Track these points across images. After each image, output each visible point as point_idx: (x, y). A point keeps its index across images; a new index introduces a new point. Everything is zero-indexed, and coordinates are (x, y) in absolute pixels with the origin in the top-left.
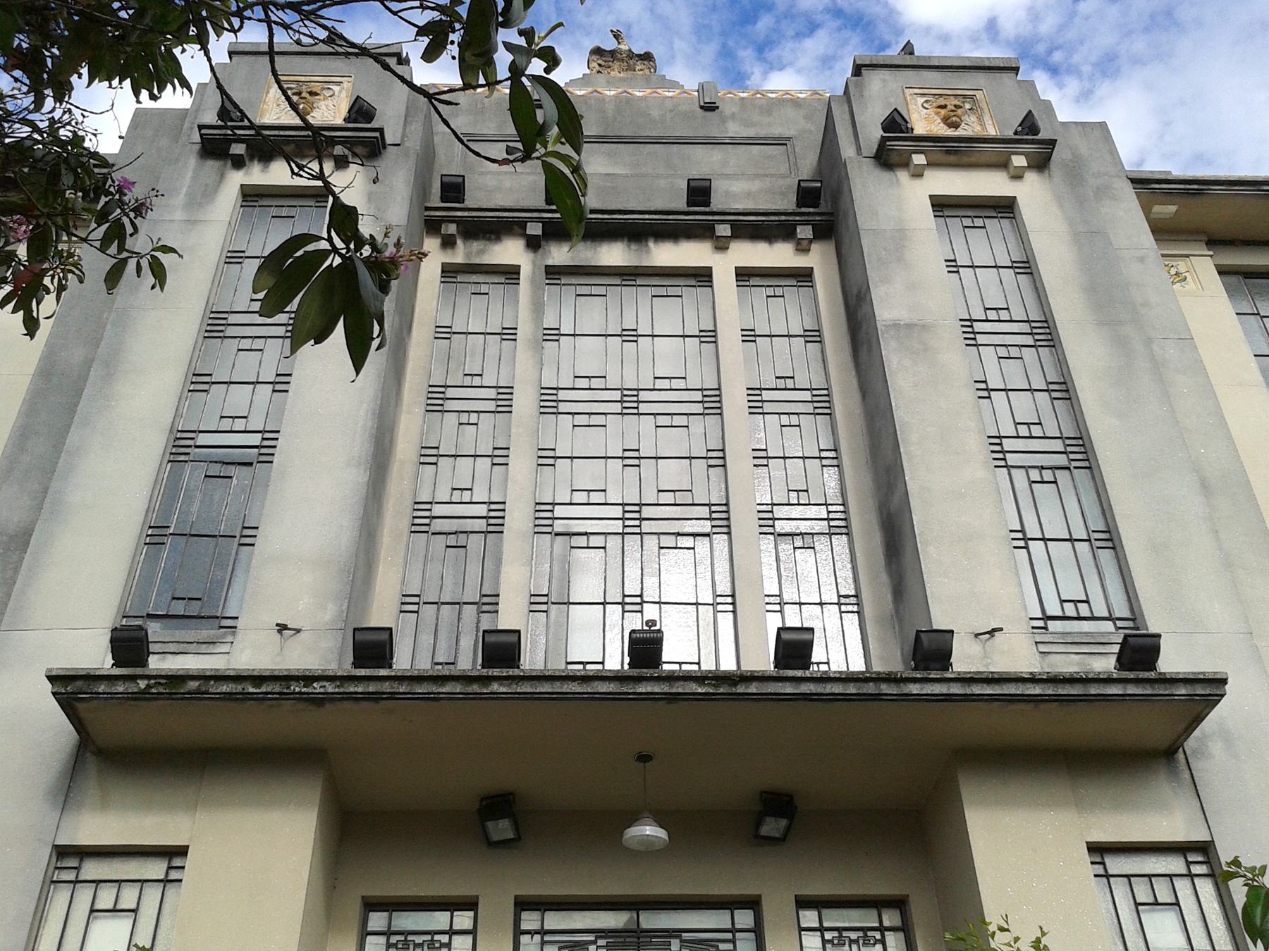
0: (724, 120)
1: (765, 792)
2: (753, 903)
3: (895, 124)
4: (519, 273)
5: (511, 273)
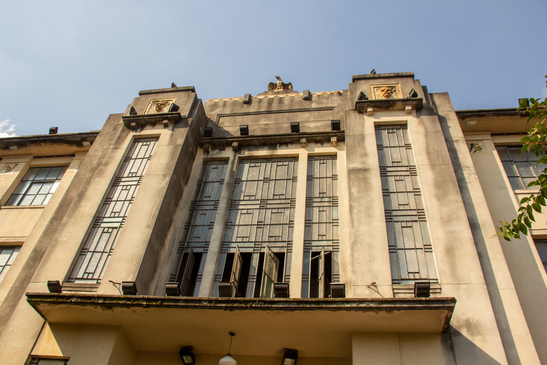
0: (311, 103)
3: (362, 96)
4: (229, 160)
5: (225, 161)
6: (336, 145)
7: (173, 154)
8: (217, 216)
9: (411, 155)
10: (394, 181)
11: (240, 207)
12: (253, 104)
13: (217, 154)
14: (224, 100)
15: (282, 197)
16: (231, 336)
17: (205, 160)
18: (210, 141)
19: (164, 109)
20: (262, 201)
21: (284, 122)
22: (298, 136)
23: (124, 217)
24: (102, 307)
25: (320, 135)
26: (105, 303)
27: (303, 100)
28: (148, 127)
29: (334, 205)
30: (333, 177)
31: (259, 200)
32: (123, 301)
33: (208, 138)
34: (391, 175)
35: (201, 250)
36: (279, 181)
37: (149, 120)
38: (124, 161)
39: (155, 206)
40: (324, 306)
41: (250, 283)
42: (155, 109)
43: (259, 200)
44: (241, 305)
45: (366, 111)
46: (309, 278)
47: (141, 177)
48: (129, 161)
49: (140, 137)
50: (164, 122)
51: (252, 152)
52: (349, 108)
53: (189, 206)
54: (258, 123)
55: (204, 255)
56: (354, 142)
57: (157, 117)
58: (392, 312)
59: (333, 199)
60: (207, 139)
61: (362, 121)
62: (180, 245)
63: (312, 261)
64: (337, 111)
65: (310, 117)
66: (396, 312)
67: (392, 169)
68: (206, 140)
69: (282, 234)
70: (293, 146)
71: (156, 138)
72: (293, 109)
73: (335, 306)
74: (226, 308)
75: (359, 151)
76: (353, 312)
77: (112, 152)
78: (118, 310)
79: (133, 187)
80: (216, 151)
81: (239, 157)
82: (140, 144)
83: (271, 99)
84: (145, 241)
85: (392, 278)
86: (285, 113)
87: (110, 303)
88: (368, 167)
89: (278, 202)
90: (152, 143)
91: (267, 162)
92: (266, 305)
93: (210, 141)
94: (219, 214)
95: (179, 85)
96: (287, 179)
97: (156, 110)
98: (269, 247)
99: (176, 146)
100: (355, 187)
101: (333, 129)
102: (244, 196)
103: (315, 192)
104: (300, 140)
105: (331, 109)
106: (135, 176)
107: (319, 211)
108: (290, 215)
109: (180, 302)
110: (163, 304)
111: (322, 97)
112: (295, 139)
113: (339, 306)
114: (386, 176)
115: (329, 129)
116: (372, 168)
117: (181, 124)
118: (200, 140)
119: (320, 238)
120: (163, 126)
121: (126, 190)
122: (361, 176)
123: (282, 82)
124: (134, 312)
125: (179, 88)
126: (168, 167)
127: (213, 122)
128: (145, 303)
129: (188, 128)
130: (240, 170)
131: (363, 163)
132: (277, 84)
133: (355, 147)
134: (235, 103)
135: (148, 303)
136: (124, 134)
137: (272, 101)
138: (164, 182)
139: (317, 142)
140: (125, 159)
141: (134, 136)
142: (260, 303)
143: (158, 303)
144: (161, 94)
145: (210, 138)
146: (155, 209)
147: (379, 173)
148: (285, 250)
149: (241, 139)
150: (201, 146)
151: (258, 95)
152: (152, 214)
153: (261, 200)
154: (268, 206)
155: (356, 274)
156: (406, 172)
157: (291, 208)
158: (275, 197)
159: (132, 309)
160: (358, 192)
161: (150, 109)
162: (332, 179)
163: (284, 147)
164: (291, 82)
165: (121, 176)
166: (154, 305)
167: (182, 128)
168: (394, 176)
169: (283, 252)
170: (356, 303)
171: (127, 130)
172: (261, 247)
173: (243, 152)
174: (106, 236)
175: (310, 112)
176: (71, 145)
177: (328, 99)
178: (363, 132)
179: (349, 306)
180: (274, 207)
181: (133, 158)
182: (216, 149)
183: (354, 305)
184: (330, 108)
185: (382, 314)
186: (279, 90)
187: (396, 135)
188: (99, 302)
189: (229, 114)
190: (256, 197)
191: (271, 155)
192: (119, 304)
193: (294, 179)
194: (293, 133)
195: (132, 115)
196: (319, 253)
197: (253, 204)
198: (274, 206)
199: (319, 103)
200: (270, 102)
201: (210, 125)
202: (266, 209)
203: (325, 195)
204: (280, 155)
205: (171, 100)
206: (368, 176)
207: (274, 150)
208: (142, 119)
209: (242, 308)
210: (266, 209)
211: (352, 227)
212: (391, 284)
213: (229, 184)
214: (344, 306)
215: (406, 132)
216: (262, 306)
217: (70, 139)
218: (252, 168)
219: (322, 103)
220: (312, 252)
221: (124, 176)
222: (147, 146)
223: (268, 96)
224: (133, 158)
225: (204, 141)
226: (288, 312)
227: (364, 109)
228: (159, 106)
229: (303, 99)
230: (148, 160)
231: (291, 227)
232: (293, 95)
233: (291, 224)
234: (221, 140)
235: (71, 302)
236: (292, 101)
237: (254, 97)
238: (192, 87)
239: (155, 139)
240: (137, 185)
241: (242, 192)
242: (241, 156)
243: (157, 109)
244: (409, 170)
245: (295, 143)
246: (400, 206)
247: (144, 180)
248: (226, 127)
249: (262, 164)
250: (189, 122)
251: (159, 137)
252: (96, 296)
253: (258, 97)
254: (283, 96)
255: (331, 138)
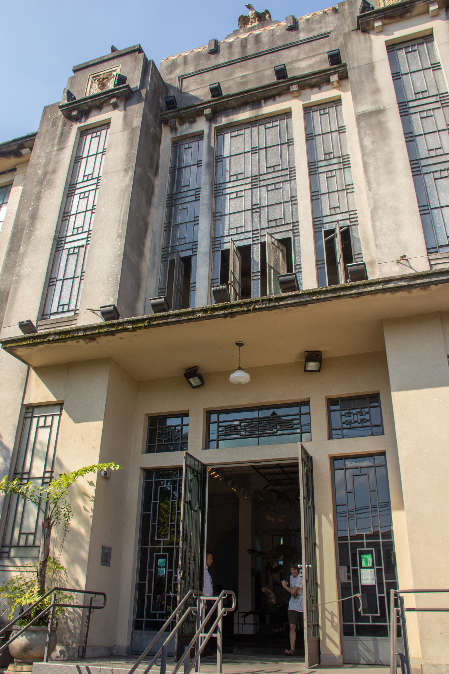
0: (299, 33)
1: (306, 352)
2: (306, 403)
4: (203, 134)
5: (199, 136)
6: (338, 86)
7: (131, 140)
8: (201, 207)
9: (440, 78)
10: (420, 120)
11: (228, 191)
12: (221, 52)
13: (187, 129)
14: (183, 54)
15: (277, 168)
16: (238, 347)
17: (174, 140)
18: (175, 114)
19: (108, 84)
20: (253, 178)
21: (266, 68)
22: (286, 84)
23: (89, 231)
24: (84, 340)
25: (315, 76)
26: (86, 335)
27: (287, 31)
28: (94, 113)
29: (345, 166)
30: (339, 130)
31: (249, 177)
32: (105, 328)
33: (171, 111)
34: (414, 112)
35: (189, 253)
36: (271, 149)
37: (93, 104)
38: (75, 163)
39: (122, 210)
40: (342, 294)
41: (255, 281)
42: (97, 87)
43: (249, 177)
44: (242, 309)
45: (373, 28)
46: (324, 264)
47: (98, 178)
48: (81, 161)
49: (86, 128)
50: (111, 102)
51: (231, 117)
52: (349, 28)
53: (166, 202)
54: (233, 77)
55: (193, 258)
56: (360, 76)
57: (101, 97)
58: (428, 289)
59: (343, 159)
60: (171, 113)
61: (369, 44)
62: (163, 251)
63: (326, 242)
64: (334, 37)
65: (299, 53)
66: (433, 287)
67: (415, 104)
68: (171, 113)
69: (284, 215)
70: (282, 98)
71: (106, 124)
72: (276, 47)
73: (355, 291)
74: (225, 316)
75: (368, 87)
76: (379, 296)
77: (57, 154)
78: (102, 340)
79: (92, 193)
80: (186, 125)
81: (215, 128)
82: (89, 137)
83: (244, 39)
84: (119, 255)
85: (426, 246)
86: (266, 56)
87: (92, 334)
88: (382, 107)
89: (274, 176)
90: (104, 132)
91: (251, 127)
92: (272, 304)
93: (175, 114)
94: (203, 205)
95: (121, 47)
96: (281, 144)
97: (99, 88)
98: (270, 234)
99: (133, 130)
100: (367, 137)
101: (332, 64)
102: (230, 176)
103: (318, 154)
104: (289, 89)
105: (326, 36)
106: (92, 179)
107: (327, 178)
108: (291, 189)
109: (171, 317)
110: (152, 324)
111: (313, 21)
112: (284, 88)
113: (360, 291)
114: (408, 115)
115: (327, 66)
116: (388, 107)
117: (134, 100)
118: (163, 115)
119: (333, 212)
120: (111, 107)
121: (84, 198)
122: (374, 121)
123: (256, 12)
124: (121, 338)
125: (121, 51)
126: (128, 159)
127: (175, 88)
128: (131, 327)
129: (144, 103)
130: (219, 145)
131: (376, 102)
132: (249, 16)
133: (362, 82)
134: (198, 56)
135: (134, 326)
136: (67, 129)
137: (246, 42)
138: (128, 179)
139: (312, 86)
140: (75, 160)
141: (79, 128)
142: (264, 303)
143: (146, 324)
144: (100, 65)
145: (174, 110)
146: (122, 214)
147: (398, 111)
148: (290, 235)
149: (213, 103)
150: (166, 122)
151: (226, 38)
152: (121, 221)
153: (252, 177)
154: (262, 183)
155: (381, 248)
156: (435, 104)
157: (290, 180)
158: (270, 170)
159: (118, 335)
160: (373, 142)
161: (90, 88)
162: (339, 133)
163: (271, 102)
164: (267, 9)
165: (76, 183)
166: (142, 327)
167: (136, 104)
168: (420, 112)
169: (289, 236)
170: (382, 284)
171: (69, 123)
172: (261, 236)
173: (219, 119)
174: (73, 258)
175: (298, 46)
176: (8, 157)
177: (320, 22)
178: (371, 59)
179: (373, 288)
180: (269, 183)
181: (84, 156)
182: (185, 123)
183: (380, 287)
184: (324, 34)
185: (416, 292)
186: (253, 25)
187: (418, 54)
188: (80, 334)
189: (193, 73)
190: (246, 175)
191: (256, 117)
192: (102, 333)
193: (290, 142)
194: (279, 81)
195: (70, 102)
196: (333, 231)
197: (242, 185)
198: (269, 182)
199: (309, 30)
200: (244, 44)
201: (171, 93)
202: (260, 187)
203: (332, 156)
204: (267, 114)
205: (115, 70)
206: (384, 120)
207: (258, 108)
208: (84, 103)
209: (244, 312)
210: (260, 187)
211: (369, 190)
212: (426, 254)
213: (208, 165)
214: (366, 290)
215: (433, 46)
216: (268, 305)
217: (4, 150)
218: (235, 138)
219: (313, 30)
220: (324, 231)
221: (78, 182)
222: (98, 138)
223: (240, 36)
224: (84, 156)
225: (167, 116)
226: (300, 308)
227: (370, 24)
228: (101, 82)
229: (287, 30)
230: (103, 155)
231: (294, 204)
232: (273, 28)
233: (293, 200)
234: (189, 110)
235: (49, 341)
236: (273, 35)
237: (222, 42)
238: (137, 46)
239: (106, 127)
240: (96, 189)
241: (227, 171)
242: (217, 125)
243: (100, 86)
244: (439, 100)
245: (284, 94)
246: (430, 152)
247: (103, 182)
248: (193, 90)
249: (246, 130)
250: (143, 94)
251: (110, 123)
252: (74, 329)
253: (227, 40)
254: (259, 32)
255: (331, 78)
